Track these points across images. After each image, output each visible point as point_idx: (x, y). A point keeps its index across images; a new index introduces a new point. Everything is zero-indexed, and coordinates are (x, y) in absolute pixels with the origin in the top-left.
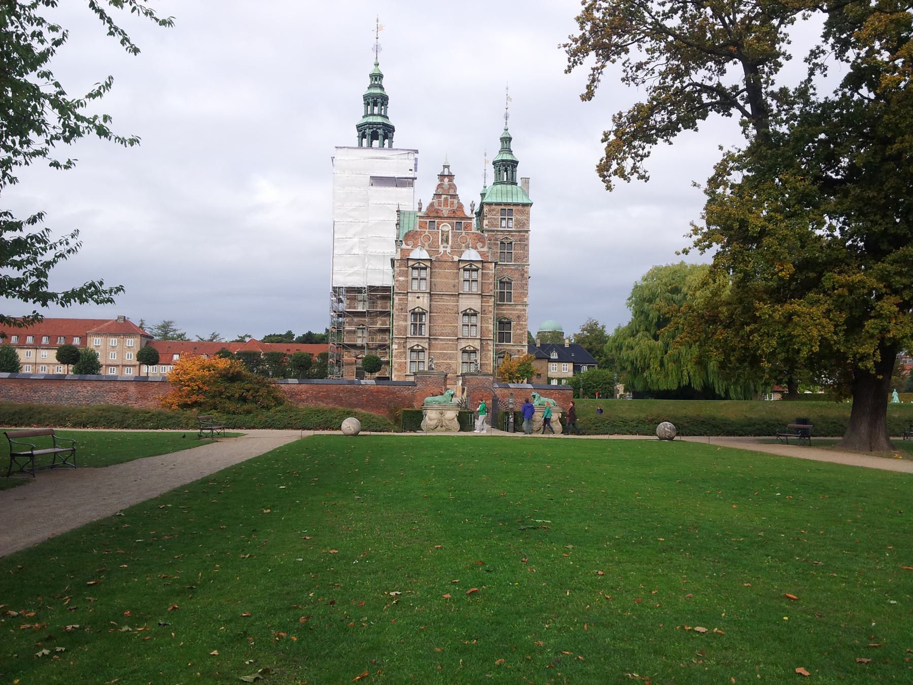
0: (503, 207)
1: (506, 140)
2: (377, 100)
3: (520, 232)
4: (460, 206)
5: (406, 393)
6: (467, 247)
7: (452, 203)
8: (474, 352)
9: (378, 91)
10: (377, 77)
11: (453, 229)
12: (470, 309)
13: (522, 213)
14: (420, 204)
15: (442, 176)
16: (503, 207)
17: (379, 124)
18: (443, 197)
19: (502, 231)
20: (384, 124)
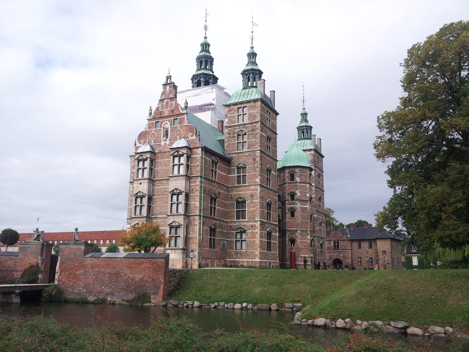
0: (239, 106)
1: (252, 55)
2: (205, 60)
3: (252, 123)
4: (177, 105)
5: (10, 263)
6: (180, 138)
7: (171, 105)
8: (179, 227)
9: (203, 53)
10: (205, 46)
11: (171, 125)
12: (176, 189)
13: (254, 107)
14: (151, 110)
15: (165, 85)
16: (239, 106)
17: (201, 74)
18: (165, 101)
19: (238, 126)
20: (204, 74)
